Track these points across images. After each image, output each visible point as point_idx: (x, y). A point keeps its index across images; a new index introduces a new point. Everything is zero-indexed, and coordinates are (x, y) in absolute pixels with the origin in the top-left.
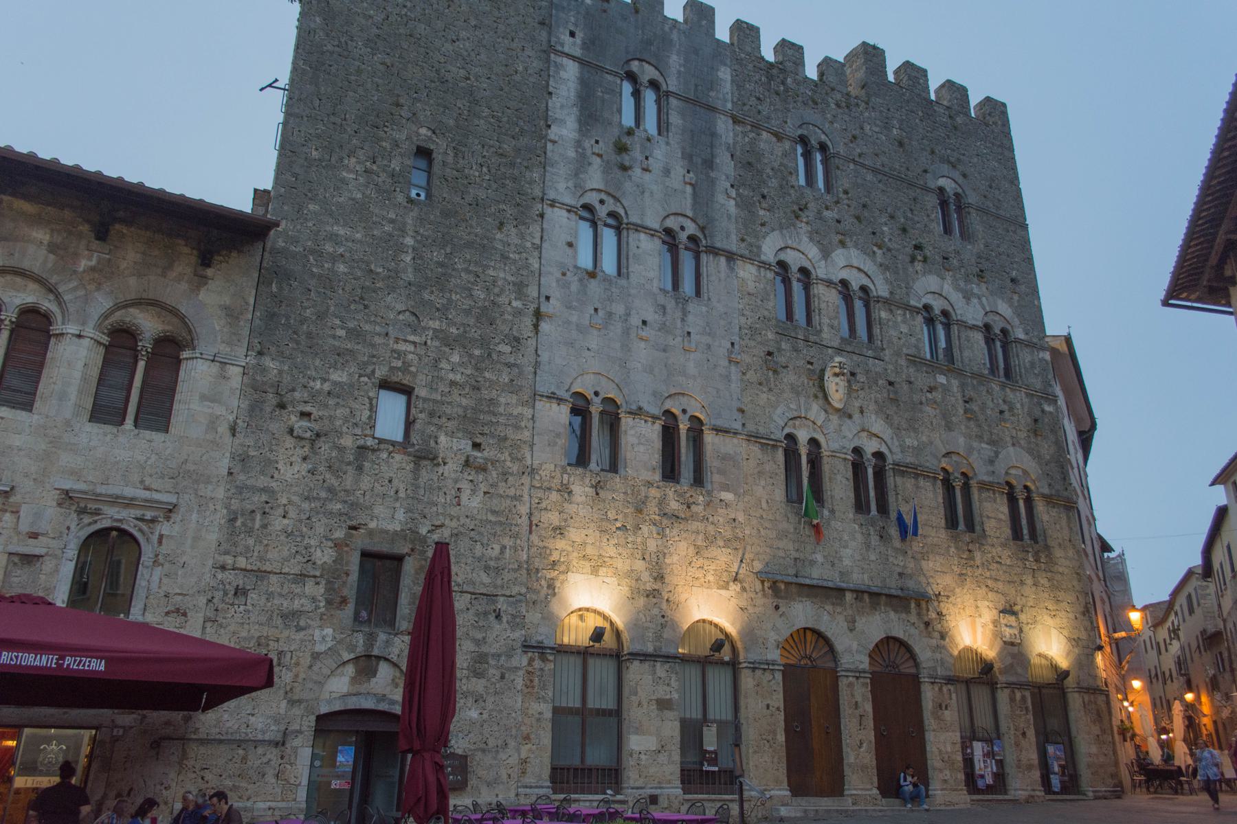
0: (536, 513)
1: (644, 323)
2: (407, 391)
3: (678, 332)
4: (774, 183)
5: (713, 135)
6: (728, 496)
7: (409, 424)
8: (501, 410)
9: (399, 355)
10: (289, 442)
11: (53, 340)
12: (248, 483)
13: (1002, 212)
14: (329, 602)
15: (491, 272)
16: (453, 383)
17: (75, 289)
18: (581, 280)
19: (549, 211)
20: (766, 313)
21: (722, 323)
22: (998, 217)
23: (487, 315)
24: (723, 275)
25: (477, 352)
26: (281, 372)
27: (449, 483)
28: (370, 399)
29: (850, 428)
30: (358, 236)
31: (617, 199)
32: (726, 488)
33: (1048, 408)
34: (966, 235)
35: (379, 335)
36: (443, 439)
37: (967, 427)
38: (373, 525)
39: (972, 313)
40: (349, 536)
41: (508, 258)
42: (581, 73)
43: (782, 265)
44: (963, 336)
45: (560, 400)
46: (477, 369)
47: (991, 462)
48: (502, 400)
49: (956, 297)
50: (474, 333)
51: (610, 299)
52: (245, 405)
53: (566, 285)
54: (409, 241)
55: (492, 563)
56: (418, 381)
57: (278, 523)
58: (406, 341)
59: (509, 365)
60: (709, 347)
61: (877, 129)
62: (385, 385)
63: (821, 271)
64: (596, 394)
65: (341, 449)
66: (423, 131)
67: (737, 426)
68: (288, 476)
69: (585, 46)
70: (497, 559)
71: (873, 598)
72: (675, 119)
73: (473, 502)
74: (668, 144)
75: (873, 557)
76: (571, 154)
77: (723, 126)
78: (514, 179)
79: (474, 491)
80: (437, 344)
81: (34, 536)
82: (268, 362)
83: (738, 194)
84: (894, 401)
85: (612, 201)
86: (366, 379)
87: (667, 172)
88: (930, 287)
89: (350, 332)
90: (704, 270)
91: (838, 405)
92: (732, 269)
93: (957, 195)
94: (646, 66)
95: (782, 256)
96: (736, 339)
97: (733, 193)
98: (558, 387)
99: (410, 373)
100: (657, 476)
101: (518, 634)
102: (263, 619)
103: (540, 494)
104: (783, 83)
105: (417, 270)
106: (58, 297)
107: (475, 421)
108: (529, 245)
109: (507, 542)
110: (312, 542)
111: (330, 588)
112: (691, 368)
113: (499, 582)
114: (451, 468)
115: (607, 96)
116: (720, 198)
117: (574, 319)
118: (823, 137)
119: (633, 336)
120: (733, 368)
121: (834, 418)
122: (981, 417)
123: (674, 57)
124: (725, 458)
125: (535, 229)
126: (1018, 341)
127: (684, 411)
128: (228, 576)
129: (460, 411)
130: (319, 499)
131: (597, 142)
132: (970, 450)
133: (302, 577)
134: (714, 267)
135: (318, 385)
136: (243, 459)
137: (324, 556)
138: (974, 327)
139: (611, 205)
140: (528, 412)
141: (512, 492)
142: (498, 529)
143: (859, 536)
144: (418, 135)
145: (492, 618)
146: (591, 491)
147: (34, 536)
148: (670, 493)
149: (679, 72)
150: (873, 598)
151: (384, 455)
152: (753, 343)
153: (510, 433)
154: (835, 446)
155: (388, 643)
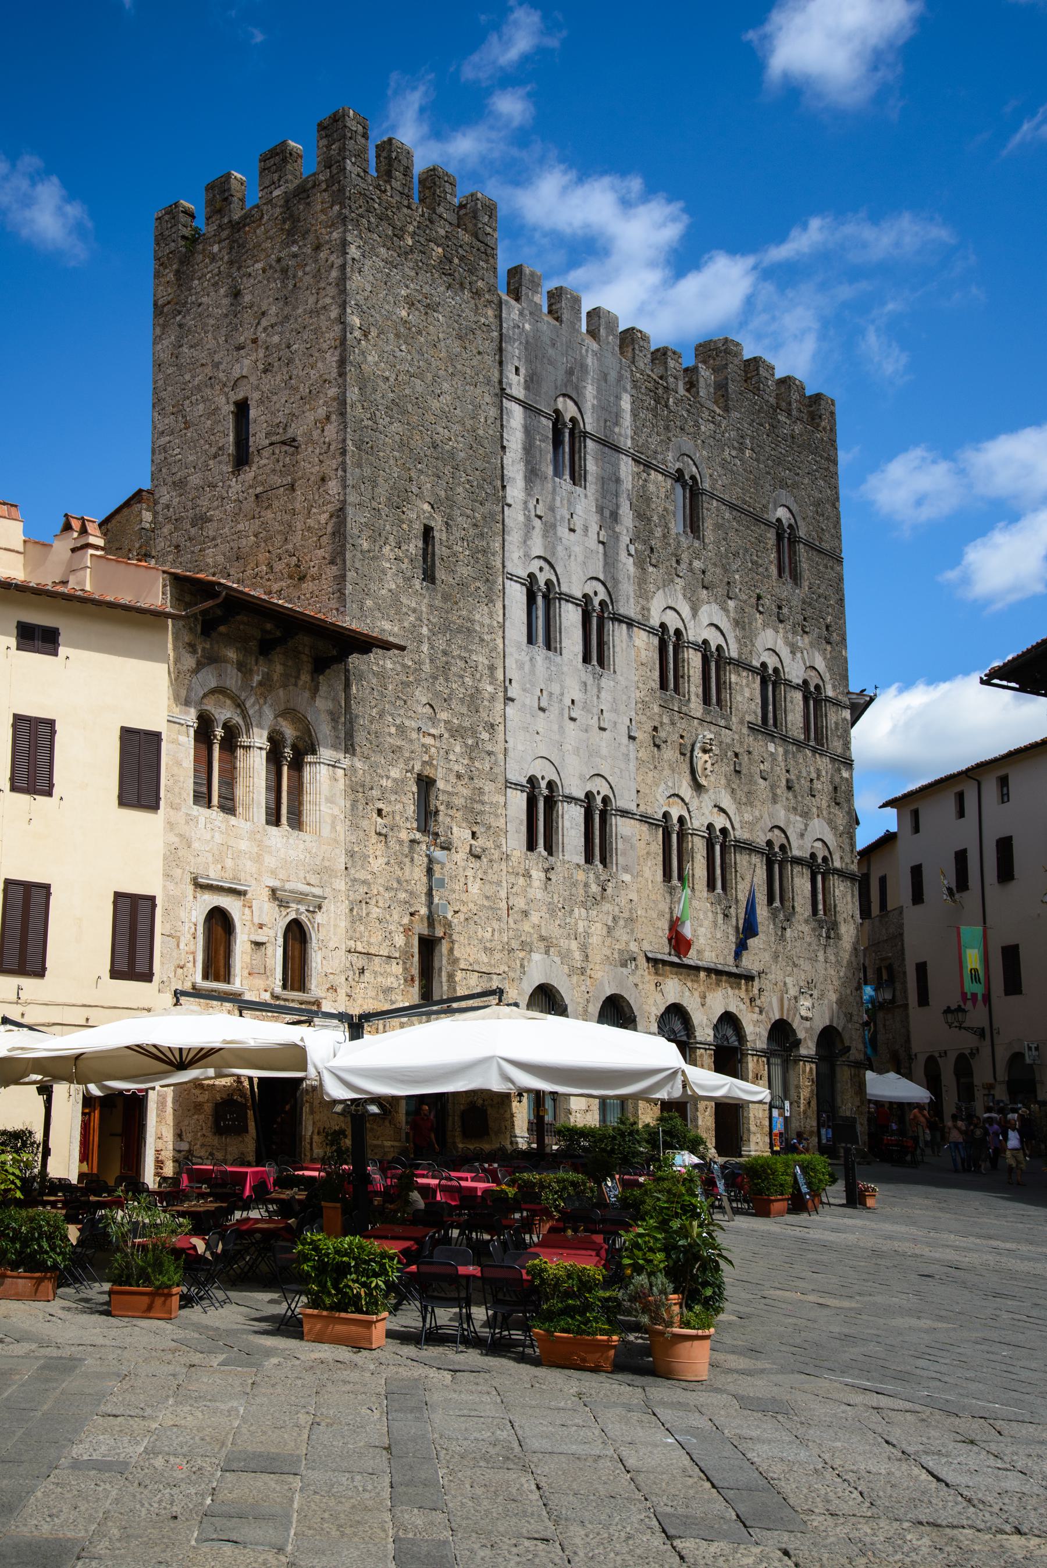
1: (573, 701)
4: (658, 532)
5: (618, 481)
6: (627, 878)
8: (486, 798)
9: (426, 748)
10: (374, 838)
11: (240, 752)
13: (824, 545)
14: (406, 980)
15: (474, 657)
16: (459, 776)
17: (253, 705)
18: (531, 660)
19: (508, 583)
22: (820, 551)
23: (473, 700)
24: (624, 645)
25: (470, 742)
29: (707, 801)
32: (626, 869)
33: (845, 774)
34: (796, 578)
35: (413, 729)
36: (455, 829)
37: (787, 799)
39: (795, 672)
40: (411, 922)
41: (483, 640)
42: (525, 418)
43: (663, 625)
44: (788, 699)
47: (802, 835)
49: (785, 652)
50: (467, 724)
51: (550, 679)
53: (521, 666)
54: (425, 631)
55: (488, 945)
57: (376, 912)
61: (734, 453)
65: (401, 842)
67: (633, 807)
68: (375, 870)
69: (527, 388)
71: (716, 973)
72: (591, 466)
73: (475, 888)
74: (586, 496)
75: (718, 936)
76: (521, 518)
78: (484, 552)
81: (261, 926)
82: (359, 765)
83: (636, 550)
84: (738, 772)
86: (409, 775)
87: (586, 529)
88: (770, 644)
90: (609, 638)
91: (703, 781)
92: (630, 637)
93: (790, 526)
94: (568, 401)
100: (582, 861)
102: (374, 994)
104: (667, 406)
106: (245, 715)
107: (472, 810)
108: (495, 624)
109: (496, 925)
110: (393, 927)
112: (604, 751)
116: (623, 555)
117: (528, 701)
118: (694, 469)
120: (632, 747)
122: (797, 787)
123: (590, 388)
126: (828, 699)
128: (354, 958)
129: (462, 801)
130: (392, 889)
132: (788, 822)
134: (618, 634)
135: (384, 782)
136: (351, 854)
137: (400, 940)
138: (797, 687)
140: (502, 800)
141: (495, 878)
143: (710, 914)
146: (542, 875)
147: (261, 926)
148: (591, 875)
149: (593, 405)
152: (644, 719)
154: (696, 824)
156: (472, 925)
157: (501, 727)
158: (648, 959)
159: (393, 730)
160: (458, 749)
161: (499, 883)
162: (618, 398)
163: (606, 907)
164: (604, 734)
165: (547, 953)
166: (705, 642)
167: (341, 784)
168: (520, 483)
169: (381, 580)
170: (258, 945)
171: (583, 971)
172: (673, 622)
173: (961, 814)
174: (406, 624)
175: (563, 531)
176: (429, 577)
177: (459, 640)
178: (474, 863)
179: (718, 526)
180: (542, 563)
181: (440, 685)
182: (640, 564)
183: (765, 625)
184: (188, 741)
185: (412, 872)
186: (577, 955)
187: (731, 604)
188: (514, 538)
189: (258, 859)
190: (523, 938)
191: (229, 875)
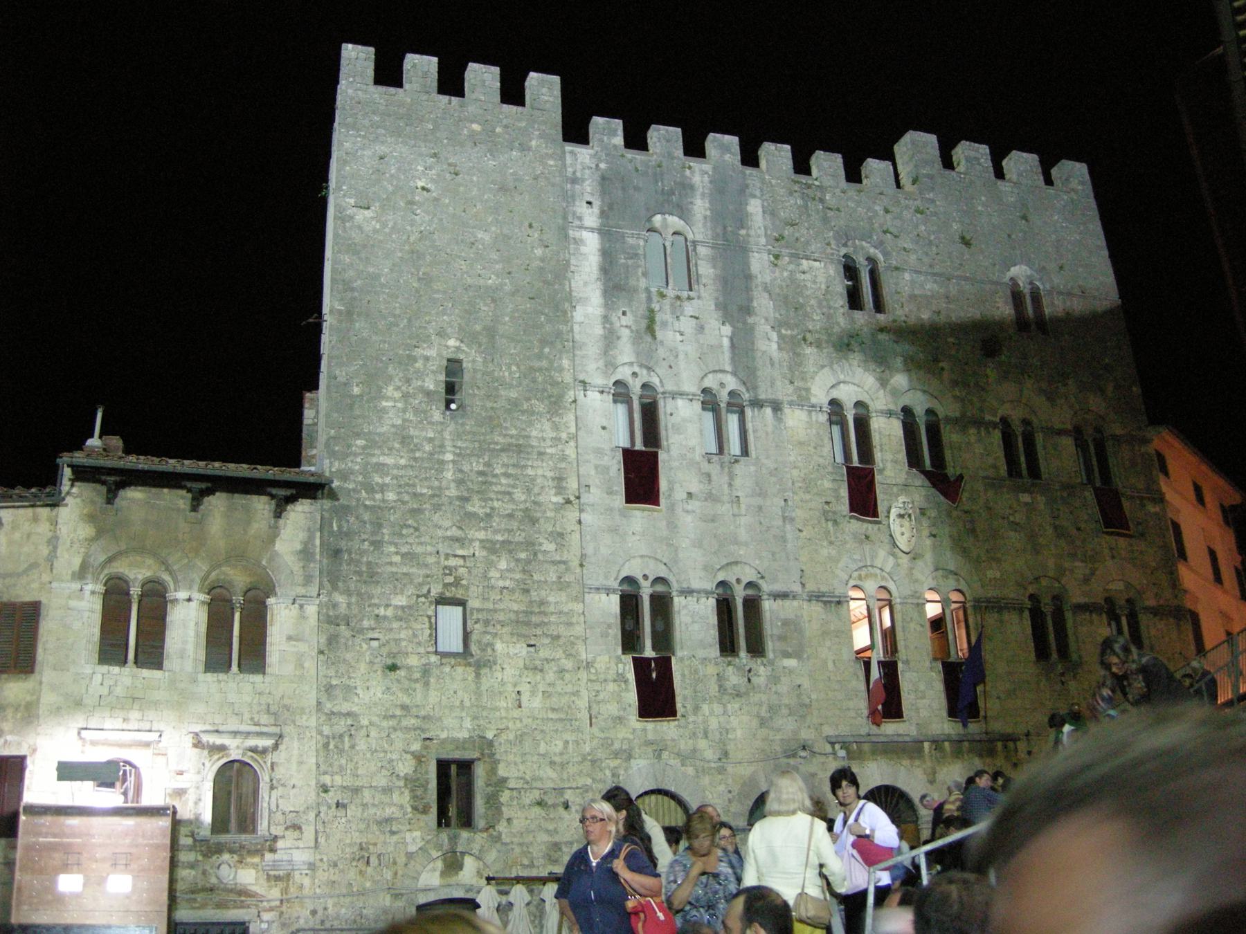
0: (594, 706)
1: (689, 494)
2: (461, 603)
3: (726, 498)
5: (749, 277)
6: (791, 663)
7: (466, 636)
9: (449, 570)
12: (335, 710)
15: (530, 472)
20: (821, 460)
21: (773, 479)
24: (770, 429)
26: (349, 605)
27: (509, 688)
28: (429, 617)
30: (403, 462)
31: (649, 369)
32: (787, 655)
35: (431, 554)
36: (499, 646)
38: (444, 735)
43: (834, 403)
45: (608, 591)
46: (524, 571)
48: (551, 599)
52: (323, 640)
54: (449, 457)
55: (557, 759)
56: (470, 593)
57: (362, 745)
58: (456, 556)
59: (554, 563)
60: (760, 508)
62: (442, 601)
64: (645, 577)
67: (797, 588)
70: (561, 754)
73: (534, 703)
79: (533, 693)
80: (484, 553)
83: (781, 337)
85: (645, 372)
86: (423, 599)
89: (403, 555)
90: (749, 426)
92: (780, 420)
95: (835, 394)
96: (789, 494)
97: (774, 336)
98: (606, 577)
99: (463, 586)
100: (715, 651)
103: (597, 687)
105: (460, 483)
108: (564, 436)
110: (394, 757)
111: (414, 797)
112: (743, 535)
113: (565, 776)
114: (510, 673)
115: (630, 262)
116: (761, 345)
119: (679, 511)
120: (788, 527)
124: (786, 623)
125: (570, 417)
127: (738, 581)
129: (513, 616)
130: (393, 716)
131: (624, 313)
133: (387, 790)
135: (382, 612)
137: (406, 767)
139: (644, 376)
140: (578, 607)
141: (569, 688)
142: (559, 726)
144: (448, 347)
145: (561, 809)
151: (447, 669)
152: (808, 497)
153: (562, 630)
155: (469, 841)
156: (528, 744)
157: (576, 536)
159: (397, 559)
160: (503, 565)
161: (576, 694)
163: (755, 698)
165: (658, 754)
167: (313, 621)
169: (380, 418)
171: (722, 770)
174: (417, 455)
178: (530, 677)
181: (476, 507)
185: (426, 697)
186: (710, 754)
190: (617, 746)
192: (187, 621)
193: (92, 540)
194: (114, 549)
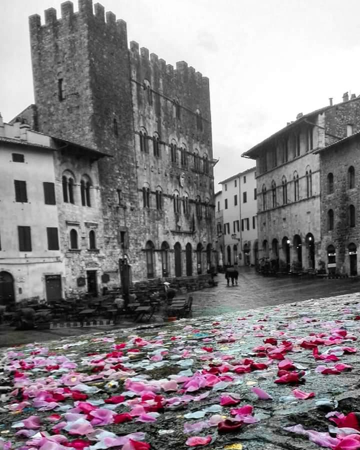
10: (108, 207)
19: (136, 135)
43: (172, 144)
63: (178, 146)
66: (114, 113)
72: (153, 100)
76: (137, 115)
77: (162, 100)
81: (84, 233)
87: (153, 118)
91: (182, 185)
100: (156, 208)
101: (140, 248)
112: (160, 179)
116: (162, 125)
121: (181, 189)
133: (114, 239)
150: (186, 233)
158: (171, 231)
162: (159, 80)
164: (160, 175)
166: (182, 148)
168: (137, 105)
170: (83, 238)
172: (174, 143)
173: (236, 186)
175: (147, 119)
176: (116, 133)
177: (125, 152)
179: (183, 115)
180: (143, 128)
182: (166, 127)
183: (195, 143)
184: (61, 185)
187: (187, 136)
188: (136, 121)
189: (81, 216)
191: (74, 221)
192: (78, 190)
193: (60, 165)
194: (65, 168)
